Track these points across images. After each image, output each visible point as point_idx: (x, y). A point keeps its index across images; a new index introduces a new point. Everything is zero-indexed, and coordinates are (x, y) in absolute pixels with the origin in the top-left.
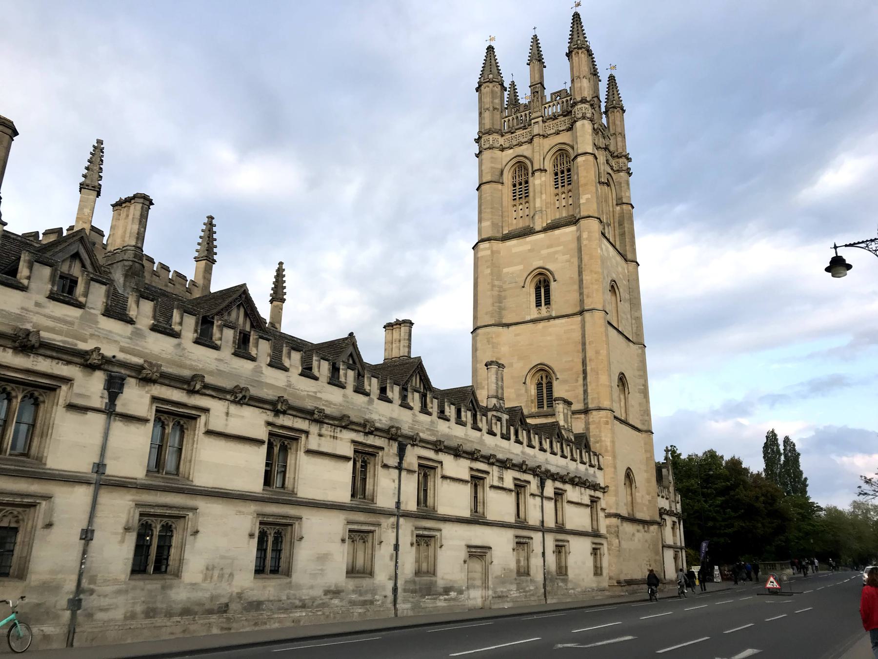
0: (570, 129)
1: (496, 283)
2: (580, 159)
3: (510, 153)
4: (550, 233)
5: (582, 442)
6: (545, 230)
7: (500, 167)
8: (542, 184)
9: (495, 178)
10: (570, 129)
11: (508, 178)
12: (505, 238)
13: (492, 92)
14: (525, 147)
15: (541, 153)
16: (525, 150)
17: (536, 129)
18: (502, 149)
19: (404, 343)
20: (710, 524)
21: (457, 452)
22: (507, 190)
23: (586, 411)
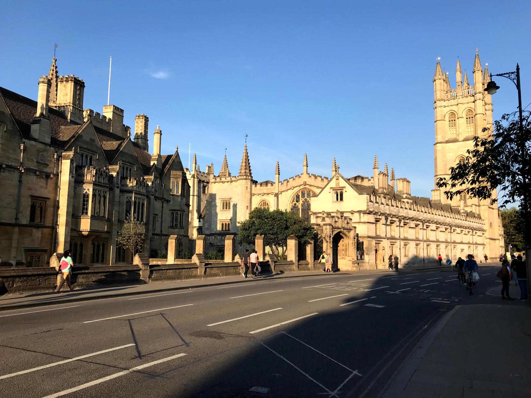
0: (474, 102)
1: (444, 159)
2: (478, 115)
3: (447, 109)
4: (465, 142)
5: (479, 217)
6: (463, 141)
7: (444, 114)
8: (462, 122)
9: (443, 119)
10: (474, 102)
11: (447, 118)
12: (447, 142)
13: (440, 83)
14: (454, 106)
15: (462, 111)
16: (455, 108)
17: (460, 101)
18: (445, 107)
19: (439, 196)
20: (513, 237)
21: (459, 227)
22: (447, 123)
23: (479, 206)
